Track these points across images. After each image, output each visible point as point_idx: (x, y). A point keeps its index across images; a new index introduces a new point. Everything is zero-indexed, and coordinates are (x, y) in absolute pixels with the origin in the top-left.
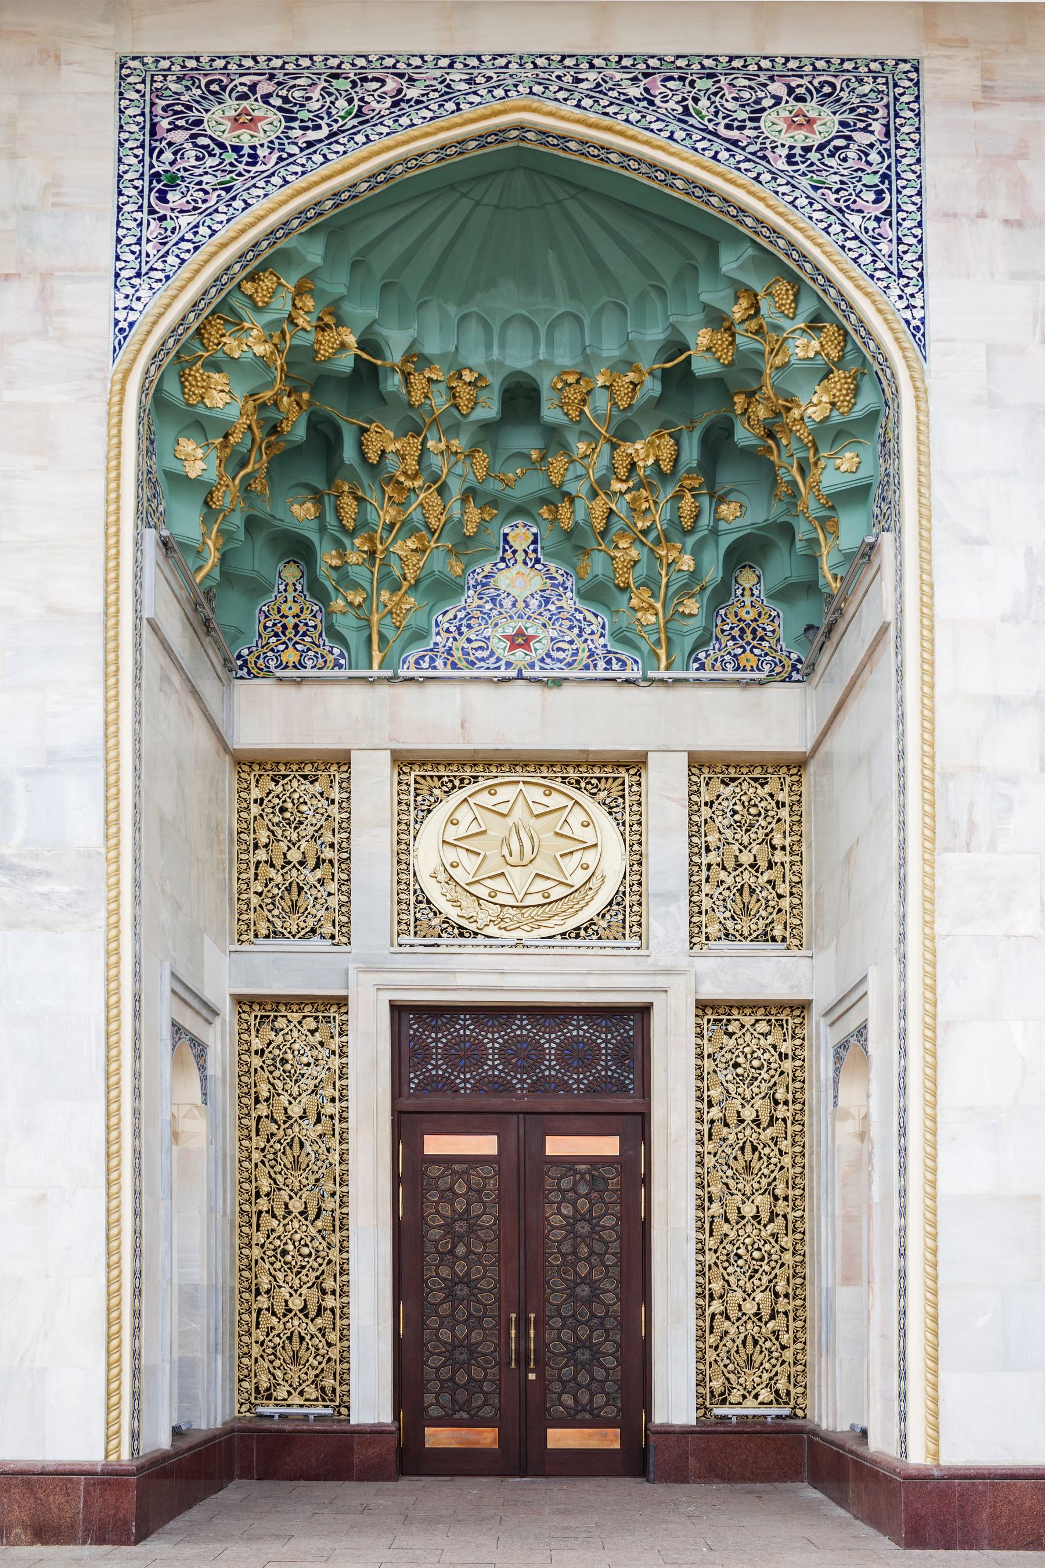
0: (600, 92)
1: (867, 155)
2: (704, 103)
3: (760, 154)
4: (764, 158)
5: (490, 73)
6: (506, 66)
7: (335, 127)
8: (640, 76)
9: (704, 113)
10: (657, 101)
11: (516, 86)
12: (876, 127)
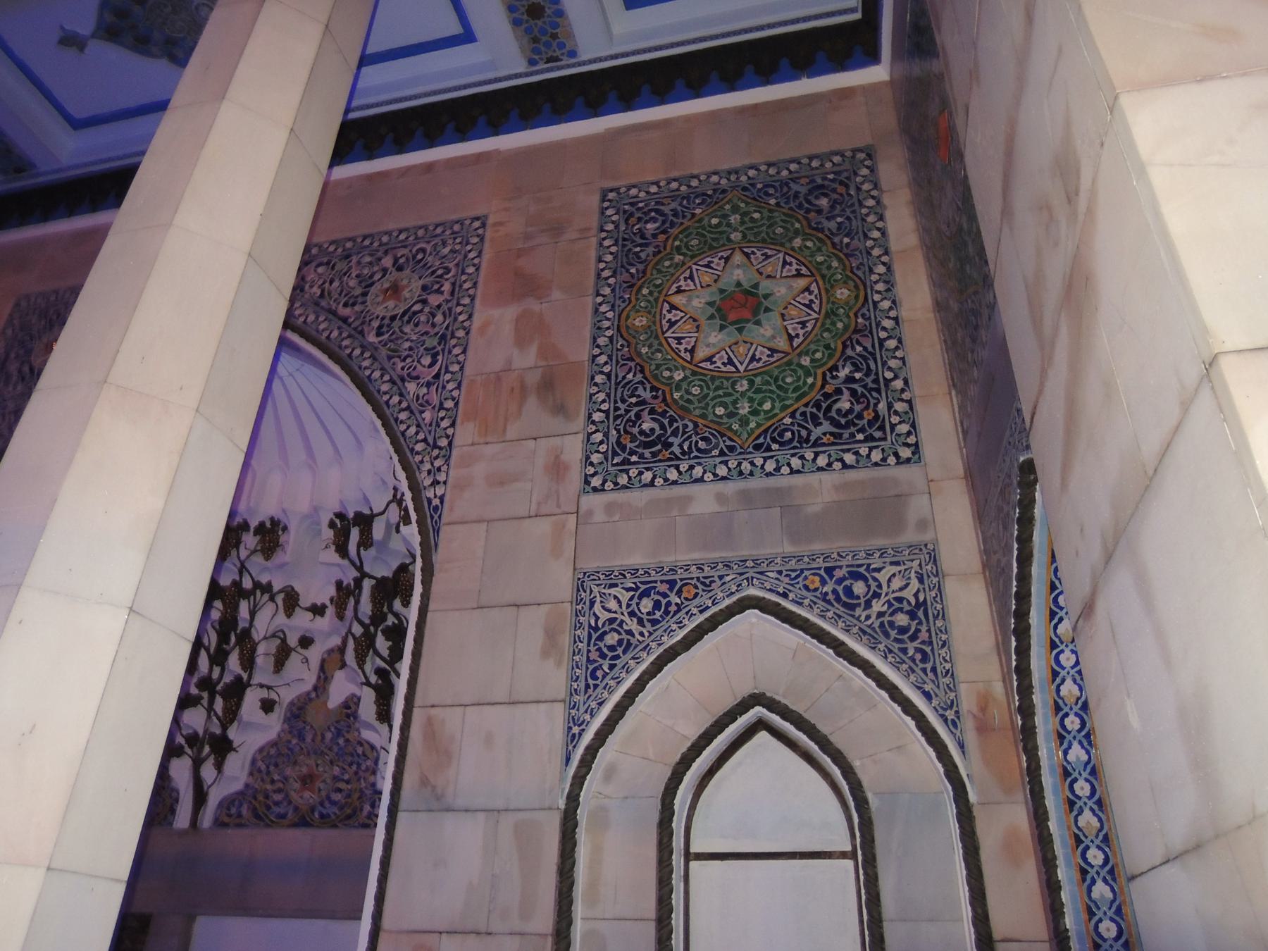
1: (434, 316)
2: (336, 284)
12: (447, 287)
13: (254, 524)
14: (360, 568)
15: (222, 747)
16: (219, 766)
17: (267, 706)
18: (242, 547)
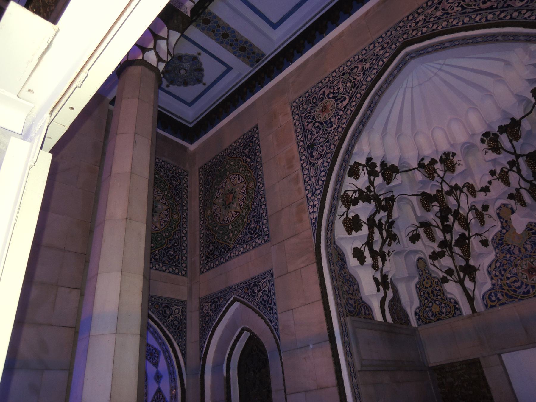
0: (427, 22)
3: (505, 5)
4: (509, 6)
5: (388, 41)
6: (391, 34)
7: (350, 96)
8: (438, 6)
9: (470, 3)
10: (450, 11)
11: (398, 40)
13: (438, 159)
14: (515, 153)
15: (470, 271)
16: (473, 279)
17: (485, 243)
18: (438, 171)
